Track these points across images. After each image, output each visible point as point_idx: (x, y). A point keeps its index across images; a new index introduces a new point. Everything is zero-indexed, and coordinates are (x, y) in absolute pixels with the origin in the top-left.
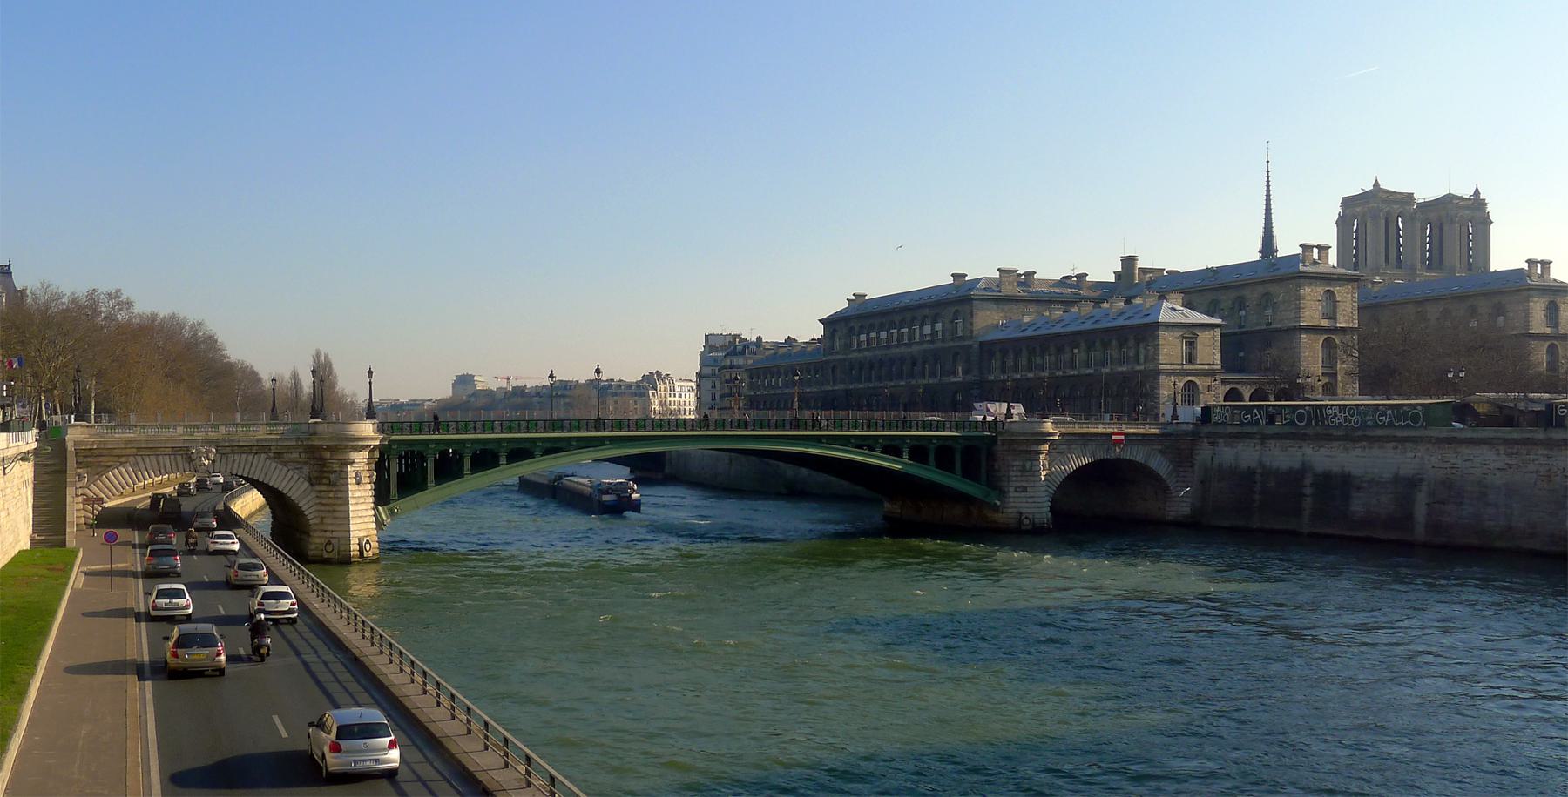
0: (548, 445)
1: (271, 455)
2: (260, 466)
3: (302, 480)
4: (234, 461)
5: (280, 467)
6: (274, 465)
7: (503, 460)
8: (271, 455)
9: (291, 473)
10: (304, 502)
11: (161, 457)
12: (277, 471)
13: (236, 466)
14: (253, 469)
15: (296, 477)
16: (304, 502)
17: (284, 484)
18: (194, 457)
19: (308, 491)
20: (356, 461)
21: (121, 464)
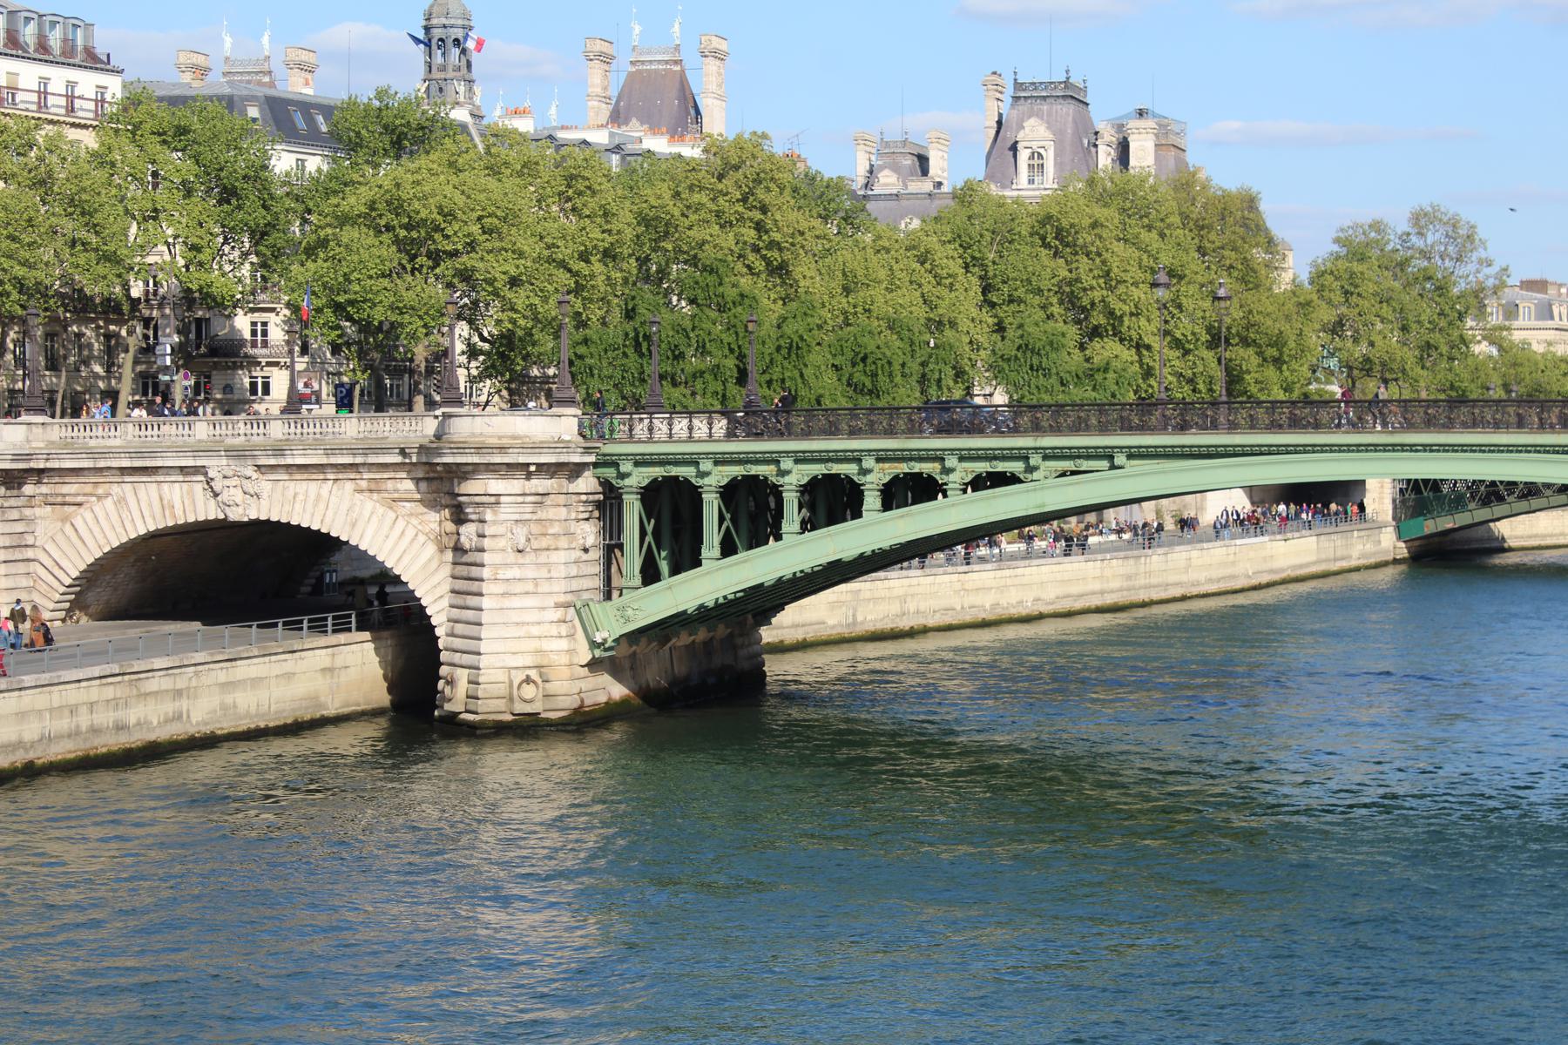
0: (982, 467)
1: (364, 484)
2: (344, 507)
3: (422, 538)
4: (319, 496)
5: (381, 510)
6: (369, 505)
7: (872, 500)
8: (364, 484)
9: (401, 524)
10: (427, 586)
11: (165, 486)
12: (375, 519)
13: (298, 507)
14: (330, 513)
15: (410, 533)
16: (427, 586)
17: (390, 543)
18: (217, 488)
19: (435, 564)
20: (503, 499)
21: (99, 498)
